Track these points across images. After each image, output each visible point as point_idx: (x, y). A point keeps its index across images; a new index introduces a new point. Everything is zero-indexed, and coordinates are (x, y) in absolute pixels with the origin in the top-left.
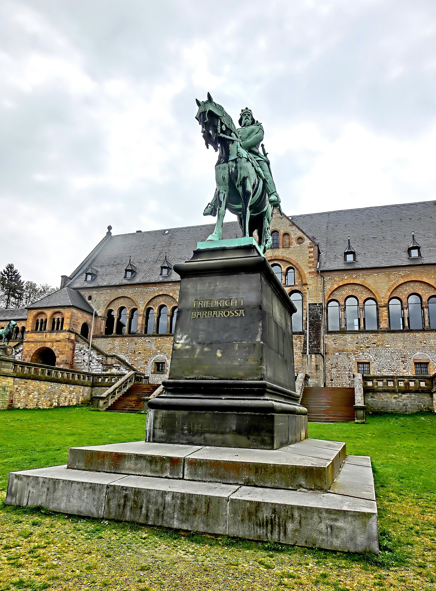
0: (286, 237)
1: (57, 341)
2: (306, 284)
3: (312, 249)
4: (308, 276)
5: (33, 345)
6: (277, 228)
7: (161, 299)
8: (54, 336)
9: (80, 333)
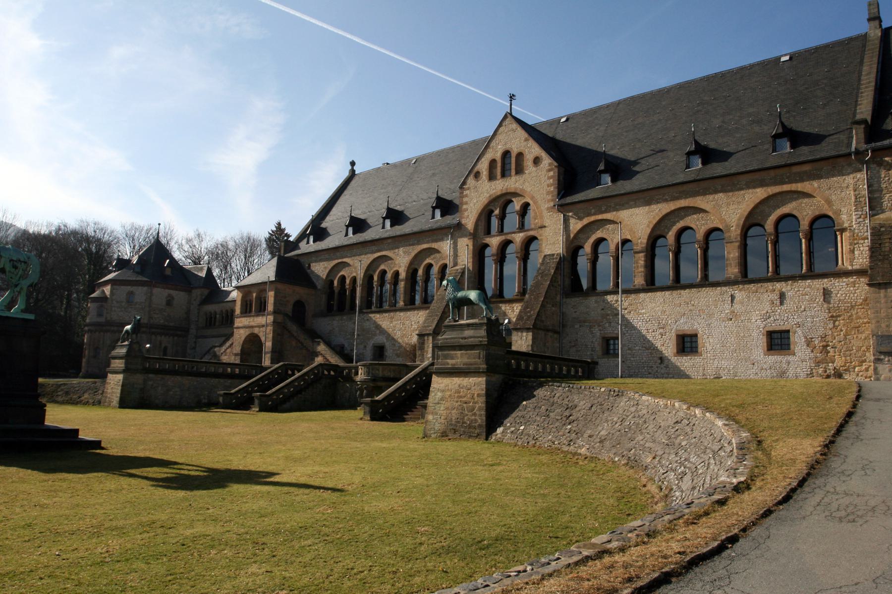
3: (551, 173)
5: (242, 331)
9: (290, 314)
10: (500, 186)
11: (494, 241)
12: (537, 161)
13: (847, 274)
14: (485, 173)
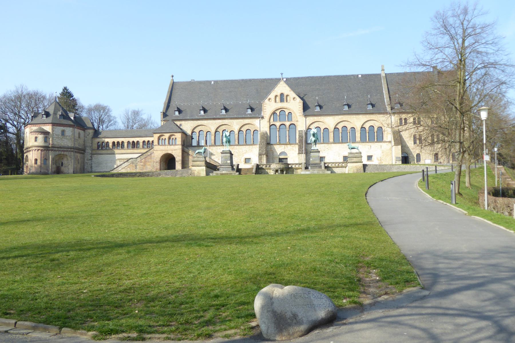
2: (297, 121)
4: (298, 117)
5: (160, 152)
6: (283, 92)
7: (223, 126)
8: (172, 147)
10: (280, 105)
11: (278, 124)
12: (294, 98)
13: (386, 142)
14: (273, 100)
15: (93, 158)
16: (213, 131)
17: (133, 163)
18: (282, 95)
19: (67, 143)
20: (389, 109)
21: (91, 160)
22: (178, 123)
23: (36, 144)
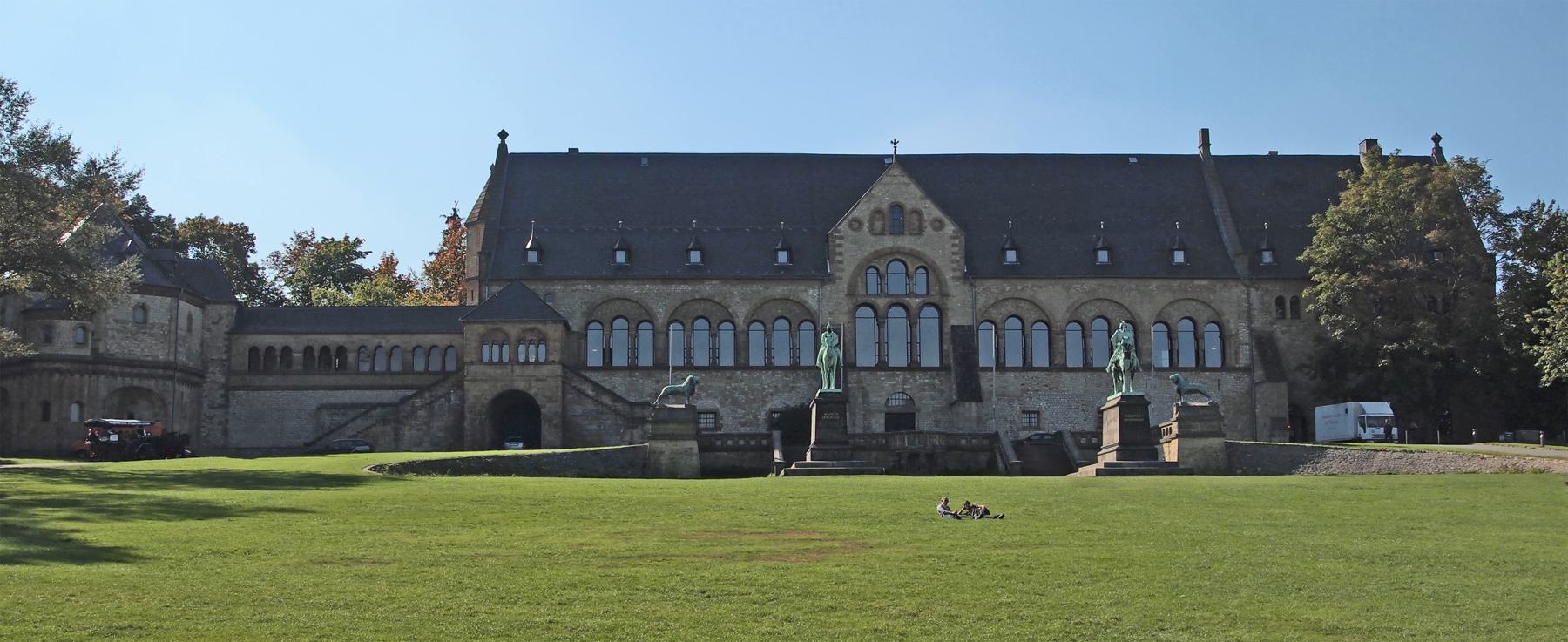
0: (915, 216)
1: (538, 380)
2: (948, 295)
4: (950, 283)
5: (486, 386)
6: (901, 200)
10: (888, 242)
15: (233, 402)
16: (661, 314)
17: (384, 421)
18: (897, 207)
19: (151, 348)
20: (1241, 265)
21: (225, 406)
22: (539, 288)
23: (48, 350)
